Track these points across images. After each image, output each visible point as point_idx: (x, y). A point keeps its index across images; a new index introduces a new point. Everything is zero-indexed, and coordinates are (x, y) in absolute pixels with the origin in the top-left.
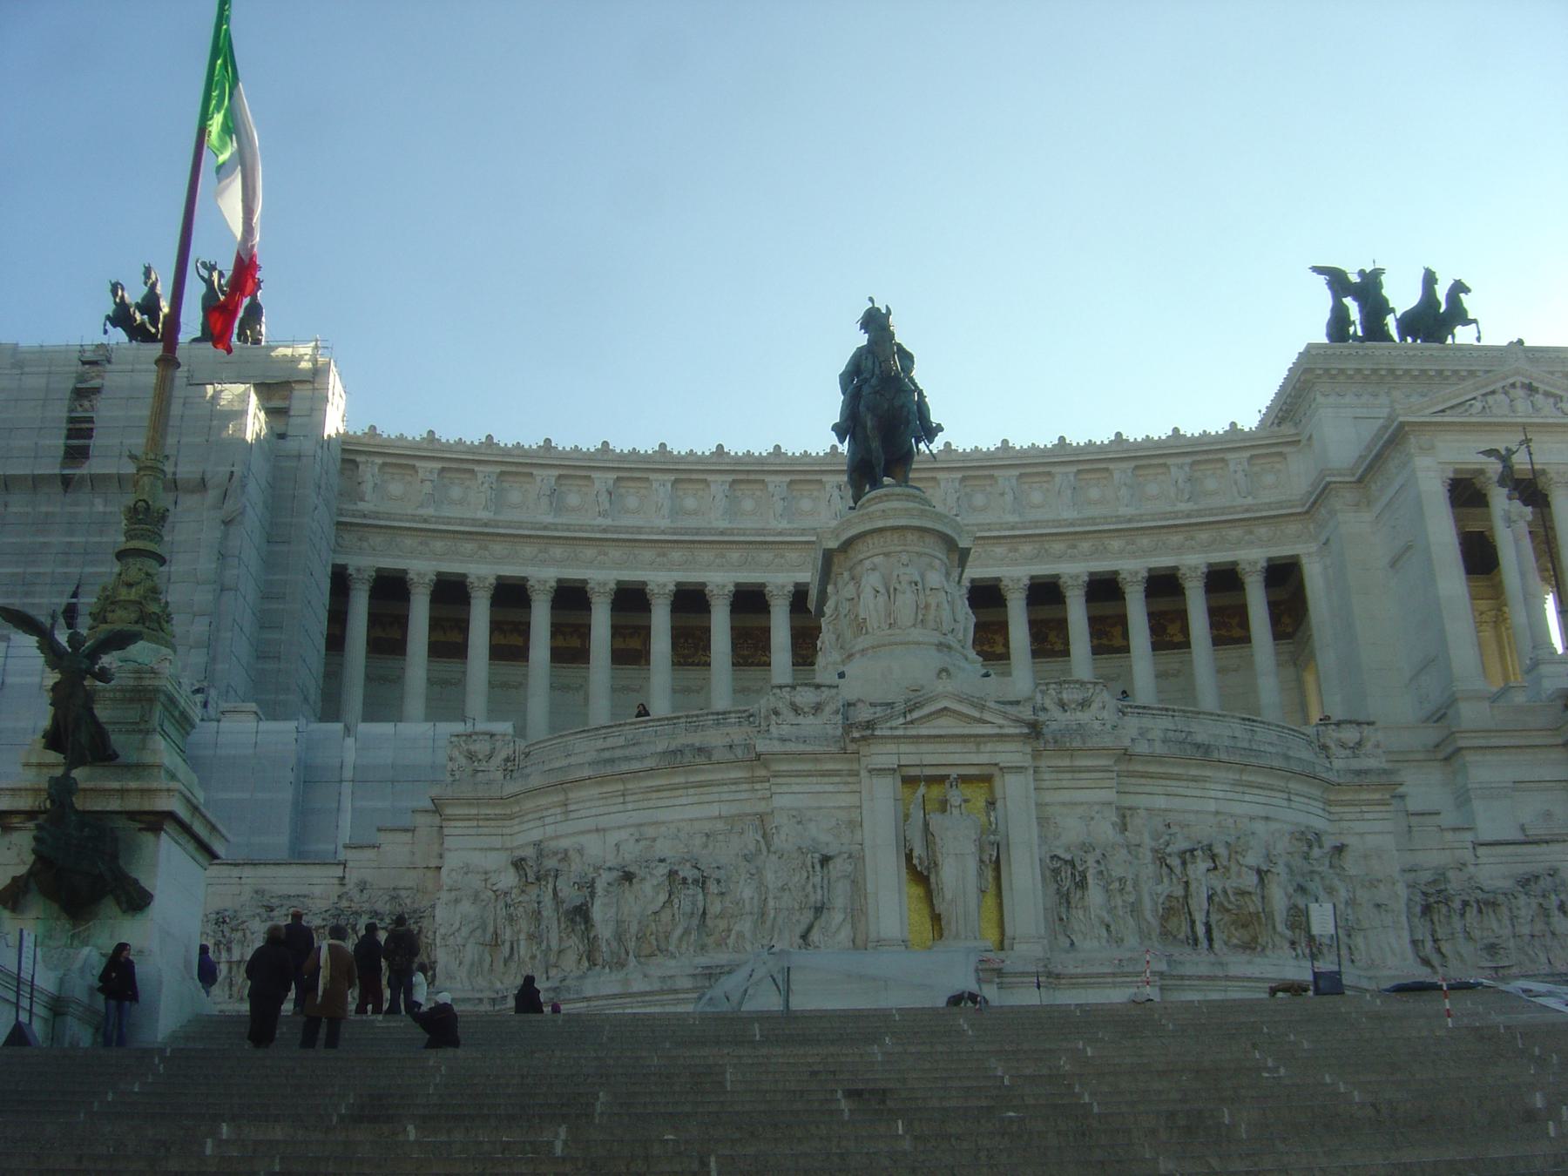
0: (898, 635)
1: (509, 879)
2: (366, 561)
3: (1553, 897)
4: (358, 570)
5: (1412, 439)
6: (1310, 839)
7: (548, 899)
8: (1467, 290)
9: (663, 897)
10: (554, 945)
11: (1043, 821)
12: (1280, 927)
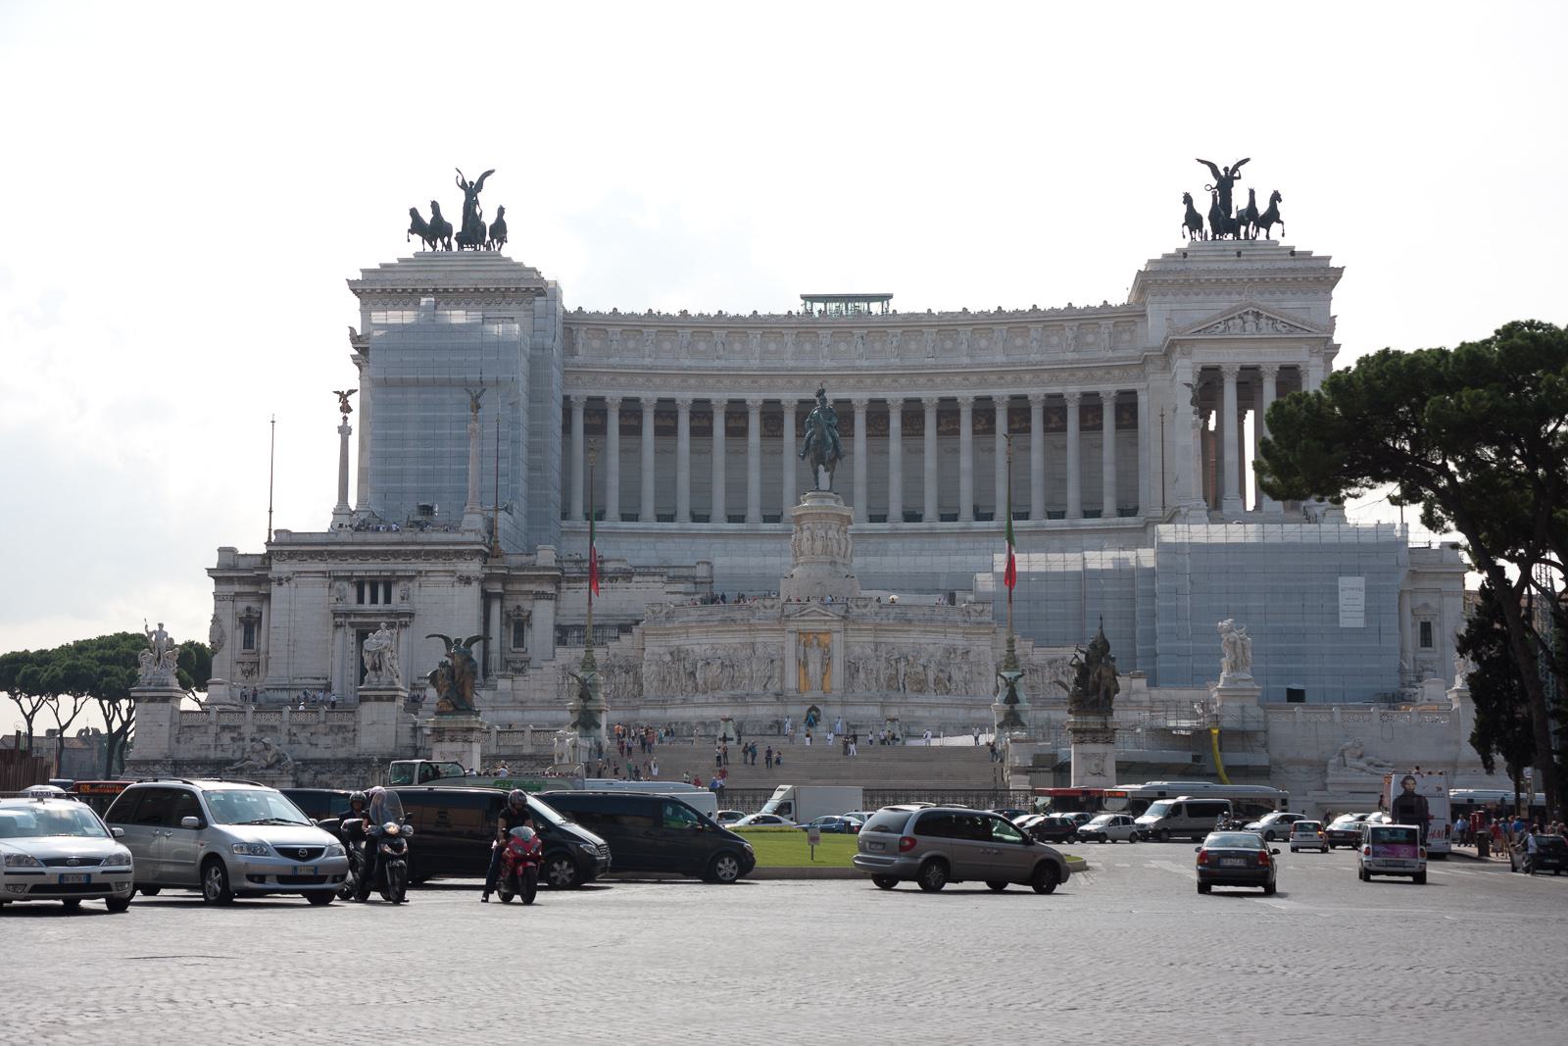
1: (668, 658)
2: (581, 393)
3: (1061, 669)
4: (576, 398)
5: (1178, 349)
7: (682, 668)
8: (1280, 201)
9: (719, 670)
11: (847, 647)
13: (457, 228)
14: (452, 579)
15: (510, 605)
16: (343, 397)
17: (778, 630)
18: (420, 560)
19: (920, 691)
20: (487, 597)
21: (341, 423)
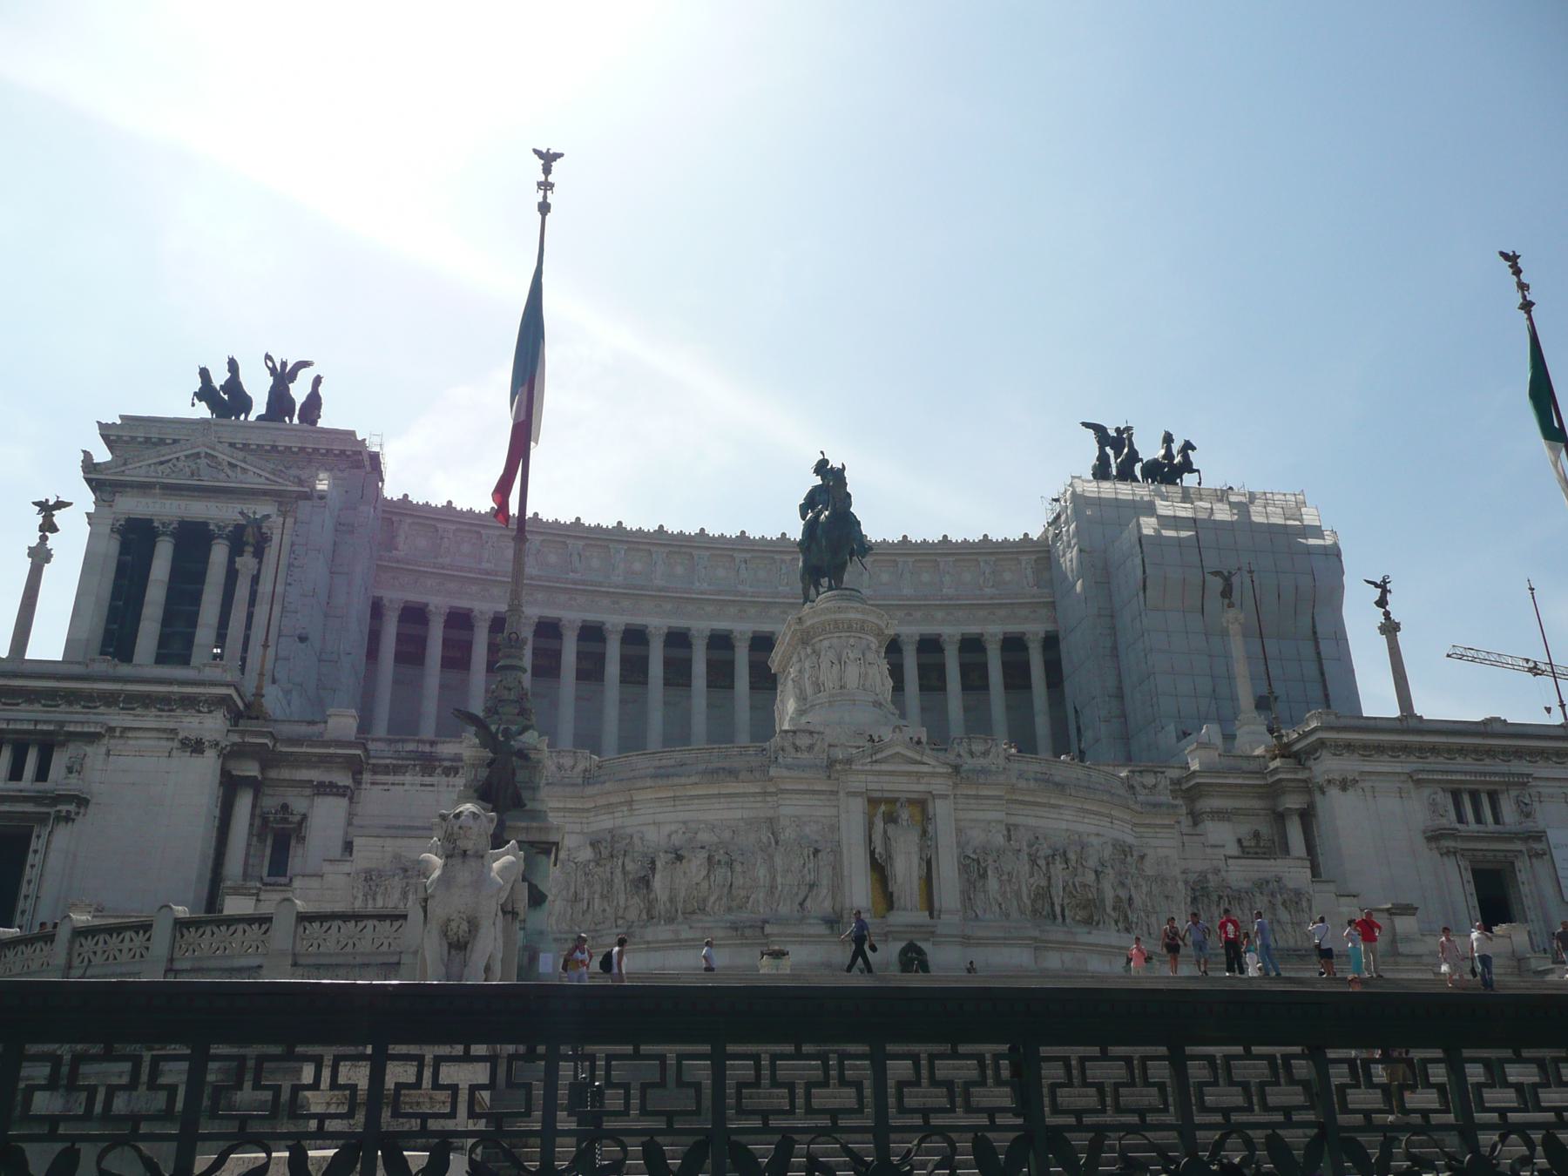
0: (828, 686)
2: (395, 596)
6: (1124, 850)
7: (618, 871)
9: (704, 873)
10: (622, 903)
11: (959, 831)
12: (1109, 910)
13: (259, 407)
14: (170, 744)
15: (270, 803)
16: (47, 509)
17: (814, 792)
18: (111, 710)
19: (1088, 922)
20: (230, 785)
21: (35, 542)
